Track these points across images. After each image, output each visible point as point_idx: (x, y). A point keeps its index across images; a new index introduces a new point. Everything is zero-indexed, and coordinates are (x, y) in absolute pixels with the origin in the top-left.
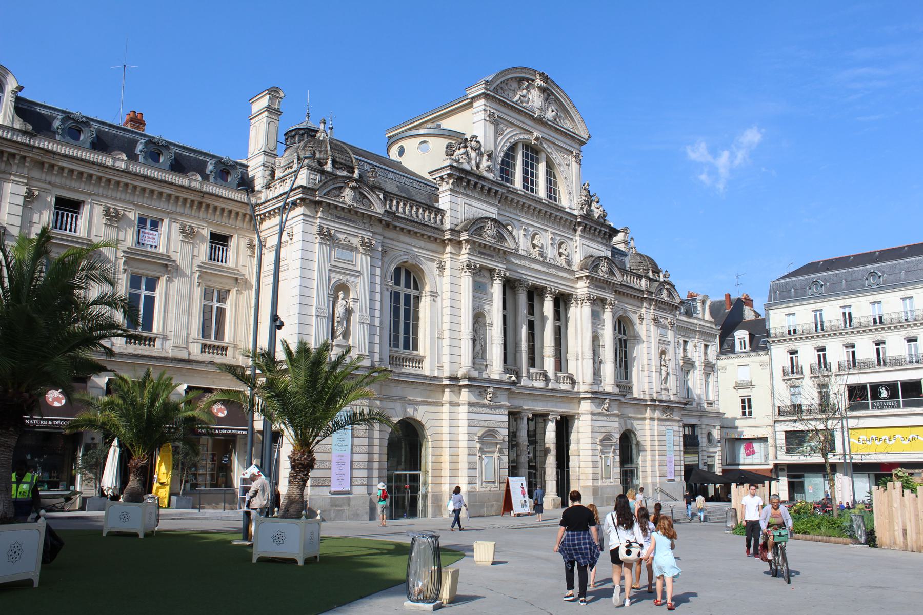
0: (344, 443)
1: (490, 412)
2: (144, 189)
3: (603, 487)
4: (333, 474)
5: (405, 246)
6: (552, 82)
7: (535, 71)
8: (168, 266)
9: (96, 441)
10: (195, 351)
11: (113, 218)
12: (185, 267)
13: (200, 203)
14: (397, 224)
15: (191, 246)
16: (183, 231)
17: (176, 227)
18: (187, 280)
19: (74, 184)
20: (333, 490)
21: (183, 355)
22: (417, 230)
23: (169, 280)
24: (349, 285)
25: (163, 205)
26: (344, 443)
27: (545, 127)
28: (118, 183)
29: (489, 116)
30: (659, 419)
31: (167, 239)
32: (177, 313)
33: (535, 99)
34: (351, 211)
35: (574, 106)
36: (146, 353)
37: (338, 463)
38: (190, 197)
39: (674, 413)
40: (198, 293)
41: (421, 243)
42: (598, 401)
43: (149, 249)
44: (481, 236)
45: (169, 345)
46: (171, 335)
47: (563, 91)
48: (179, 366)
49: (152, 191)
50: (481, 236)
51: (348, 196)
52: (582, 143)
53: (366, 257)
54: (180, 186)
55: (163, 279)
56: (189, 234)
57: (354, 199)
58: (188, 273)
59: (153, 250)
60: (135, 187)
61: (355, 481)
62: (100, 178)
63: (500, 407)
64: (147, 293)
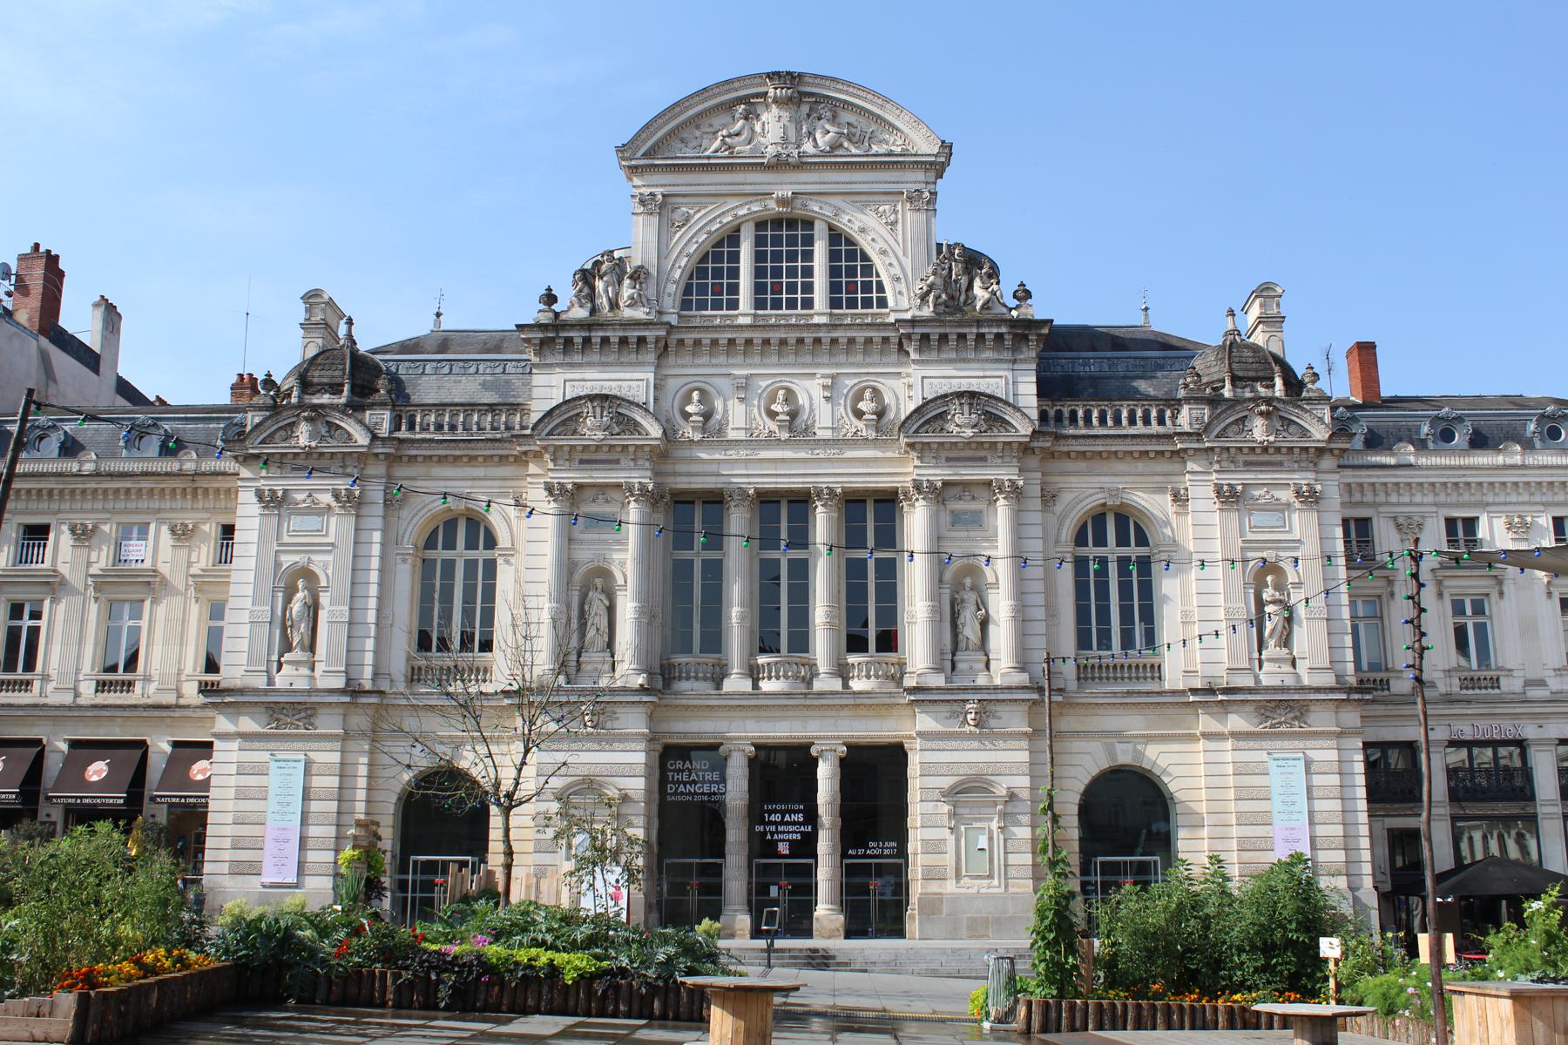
0: (289, 809)
1: (596, 746)
2: (117, 491)
3: (955, 898)
4: (268, 857)
5: (442, 483)
6: (816, 76)
7: (760, 75)
8: (151, 584)
9: (53, 819)
10: (191, 693)
11: (83, 535)
12: (179, 581)
13: (196, 489)
14: (414, 452)
15: (186, 551)
16: (173, 531)
17: (165, 529)
18: (179, 599)
19: (33, 505)
20: (267, 880)
21: (170, 699)
22: (458, 453)
23: (155, 601)
24: (313, 567)
25: (143, 504)
26: (289, 809)
27: (810, 171)
28: (84, 491)
29: (642, 202)
30: (1236, 735)
31: (155, 550)
32: (166, 642)
33: (772, 126)
34: (309, 453)
35: (888, 100)
36: (118, 702)
37: (277, 840)
38: (178, 484)
39: (1312, 718)
40: (194, 609)
41: (480, 472)
42: (947, 707)
43: (133, 566)
44: (575, 432)
45: (152, 687)
46: (155, 674)
47: (849, 84)
48: (157, 713)
49: (128, 491)
50: (575, 432)
51: (303, 436)
52: (937, 167)
53: (346, 519)
54: (167, 474)
55: (147, 603)
56: (182, 534)
57: (311, 437)
58: (182, 587)
59: (139, 566)
60: (106, 490)
61: (308, 869)
62: (62, 491)
63: (624, 738)
64: (131, 623)
